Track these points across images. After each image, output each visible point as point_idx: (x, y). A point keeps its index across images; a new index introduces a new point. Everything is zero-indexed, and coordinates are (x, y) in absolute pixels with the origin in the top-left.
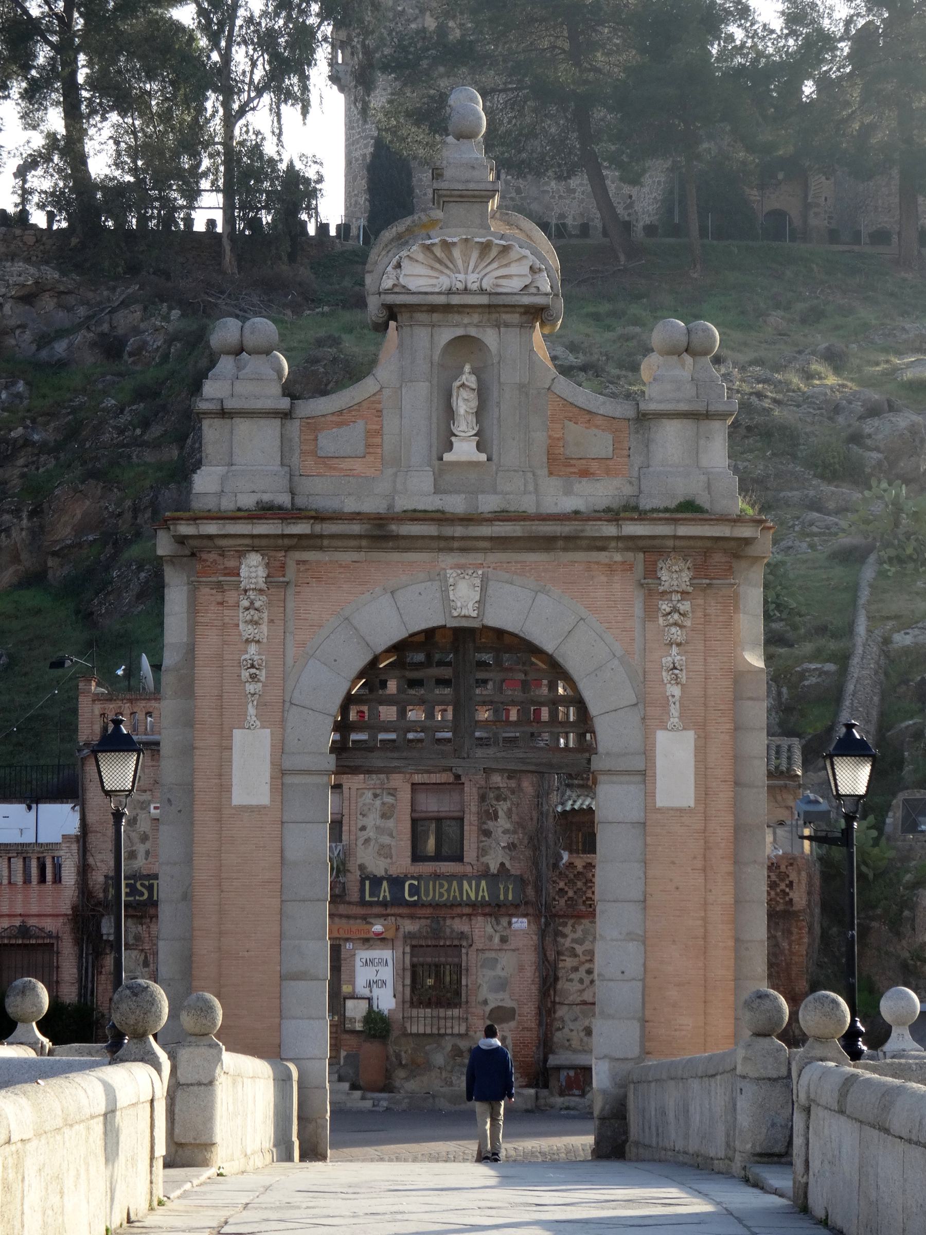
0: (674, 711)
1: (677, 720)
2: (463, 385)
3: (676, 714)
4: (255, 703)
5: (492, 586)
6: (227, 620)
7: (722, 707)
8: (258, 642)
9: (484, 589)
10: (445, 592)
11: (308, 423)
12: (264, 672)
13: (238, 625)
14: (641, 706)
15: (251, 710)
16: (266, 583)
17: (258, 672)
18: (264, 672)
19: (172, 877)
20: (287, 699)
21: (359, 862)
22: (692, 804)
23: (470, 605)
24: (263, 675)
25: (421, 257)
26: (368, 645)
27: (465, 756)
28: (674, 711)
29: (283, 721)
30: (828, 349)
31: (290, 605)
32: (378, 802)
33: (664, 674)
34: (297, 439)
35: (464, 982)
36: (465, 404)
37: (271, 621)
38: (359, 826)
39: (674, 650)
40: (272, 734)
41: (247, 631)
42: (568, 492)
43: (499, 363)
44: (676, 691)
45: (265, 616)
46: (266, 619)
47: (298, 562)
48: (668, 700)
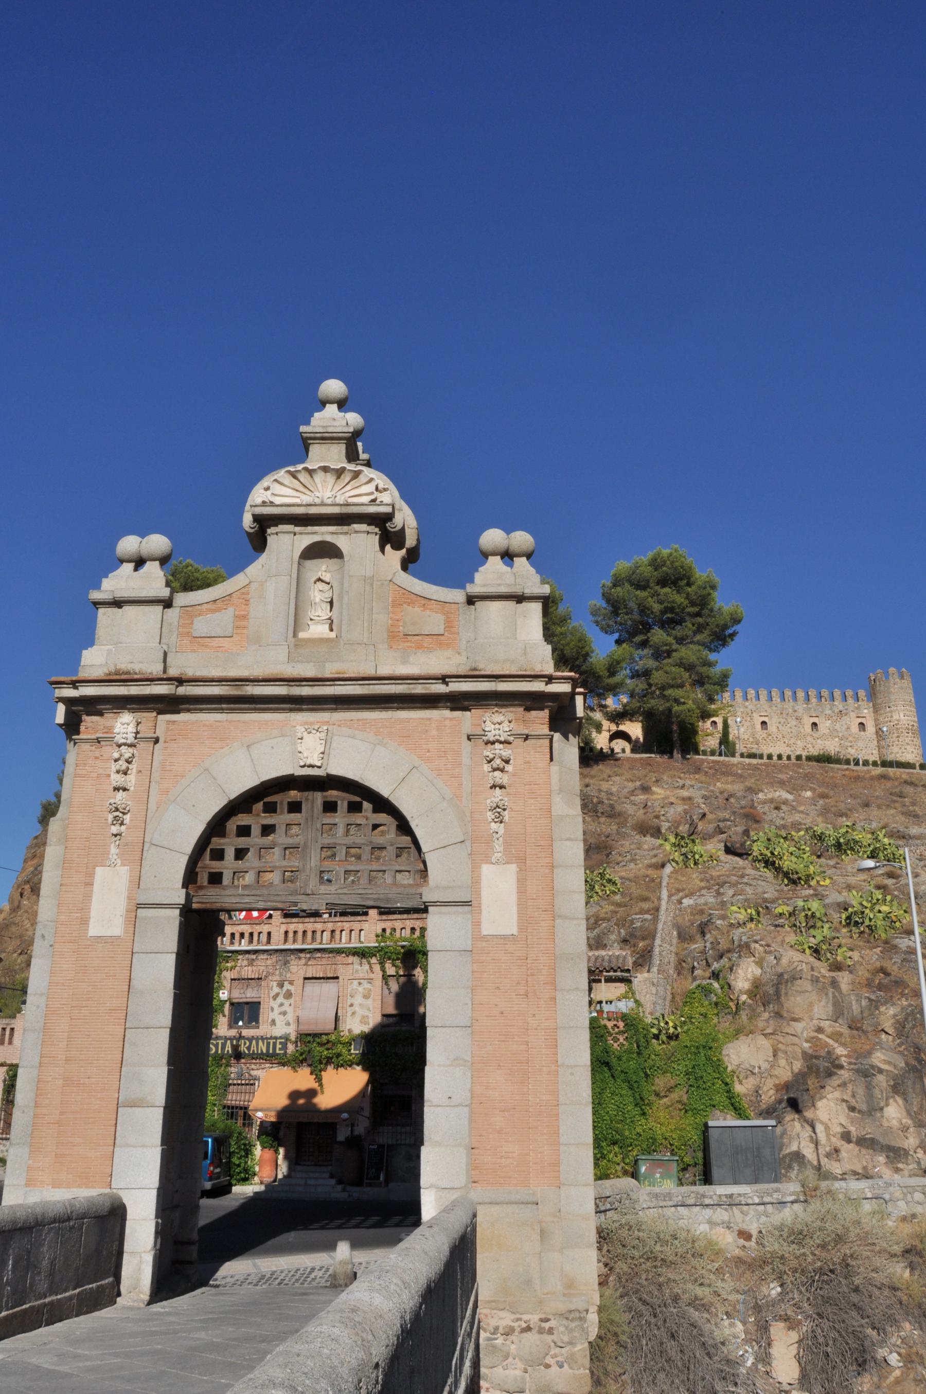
0: (498, 846)
3: (501, 849)
6: (101, 771)
7: (542, 843)
9: (327, 742)
11: (187, 611)
13: (109, 776)
14: (468, 843)
15: (113, 850)
19: (38, 1007)
21: (348, 1027)
22: (515, 931)
24: (127, 818)
28: (498, 846)
30: (641, 785)
32: (360, 989)
33: (489, 813)
35: (413, 1108)
36: (317, 594)
38: (349, 1004)
41: (117, 779)
42: (405, 661)
44: (501, 828)
46: (134, 771)
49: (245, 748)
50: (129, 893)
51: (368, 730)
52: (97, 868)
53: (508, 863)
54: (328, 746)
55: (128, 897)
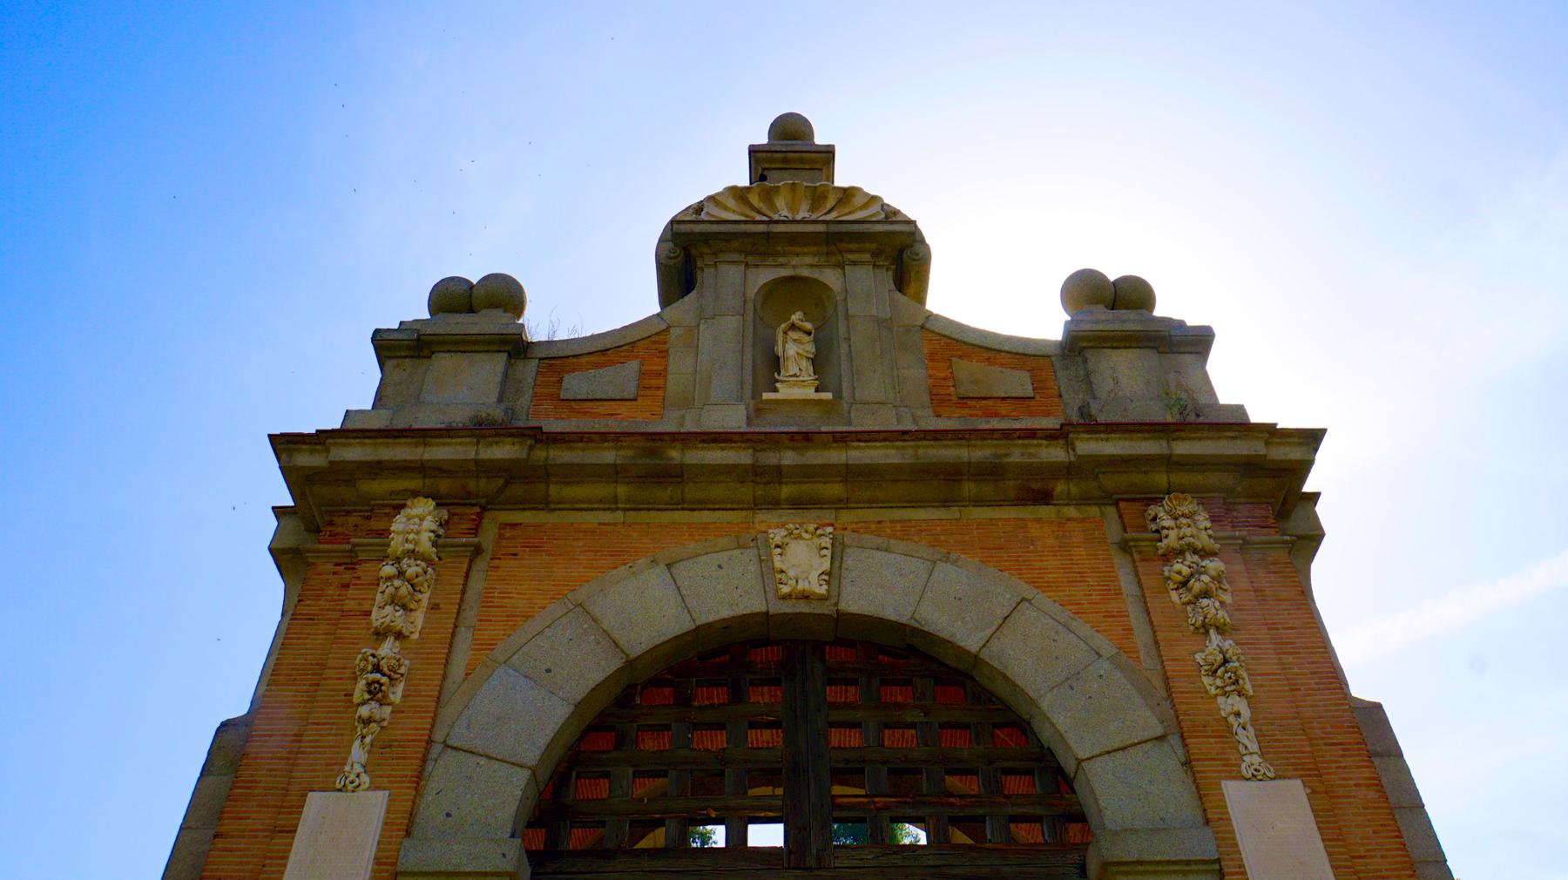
1: (1256, 759)
2: (793, 327)
3: (1254, 747)
4: (368, 740)
5: (853, 558)
7: (1339, 738)
8: (399, 636)
9: (838, 551)
10: (764, 562)
11: (551, 365)
12: (400, 688)
15: (358, 753)
16: (435, 544)
17: (384, 680)
18: (400, 688)
20: (439, 736)
23: (814, 577)
24: (397, 694)
25: (731, 203)
26: (617, 646)
27: (813, 863)
28: (1247, 739)
29: (419, 778)
31: (477, 584)
33: (1206, 680)
34: (530, 380)
37: (434, 607)
39: (1214, 637)
40: (391, 800)
41: (383, 615)
43: (845, 299)
45: (425, 598)
46: (425, 603)
47: (503, 526)
48: (1230, 726)
49: (663, 567)
50: (379, 849)
51: (916, 538)
52: (310, 794)
53: (1280, 777)
54: (837, 564)
55: (376, 858)
